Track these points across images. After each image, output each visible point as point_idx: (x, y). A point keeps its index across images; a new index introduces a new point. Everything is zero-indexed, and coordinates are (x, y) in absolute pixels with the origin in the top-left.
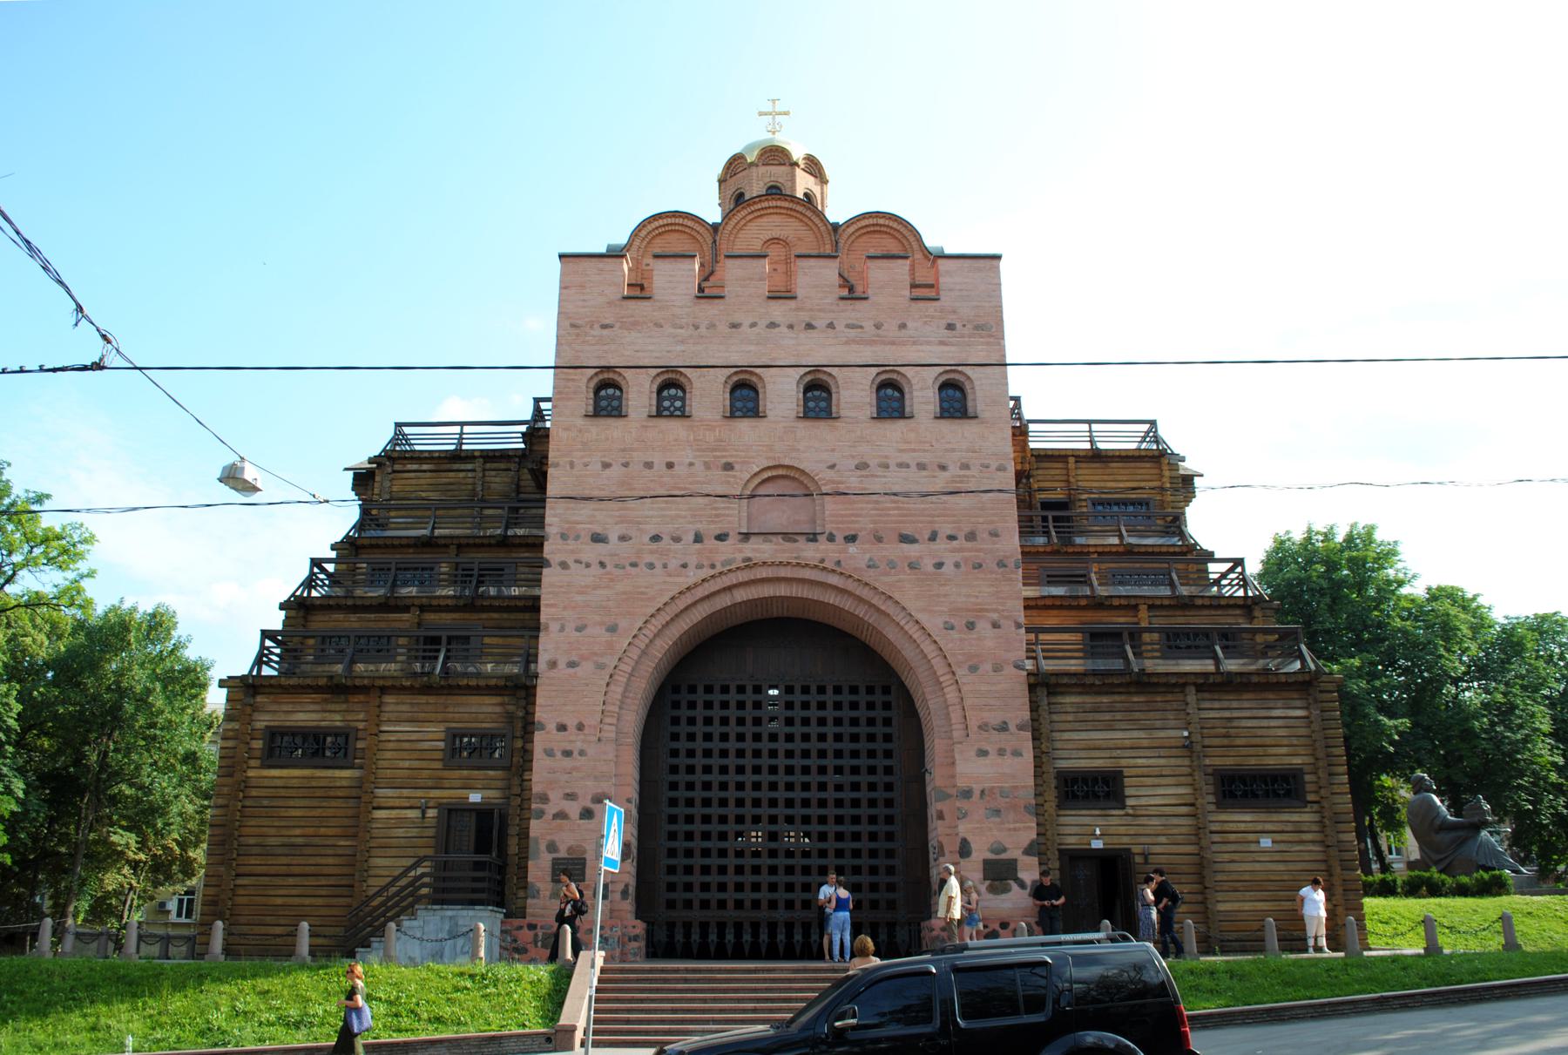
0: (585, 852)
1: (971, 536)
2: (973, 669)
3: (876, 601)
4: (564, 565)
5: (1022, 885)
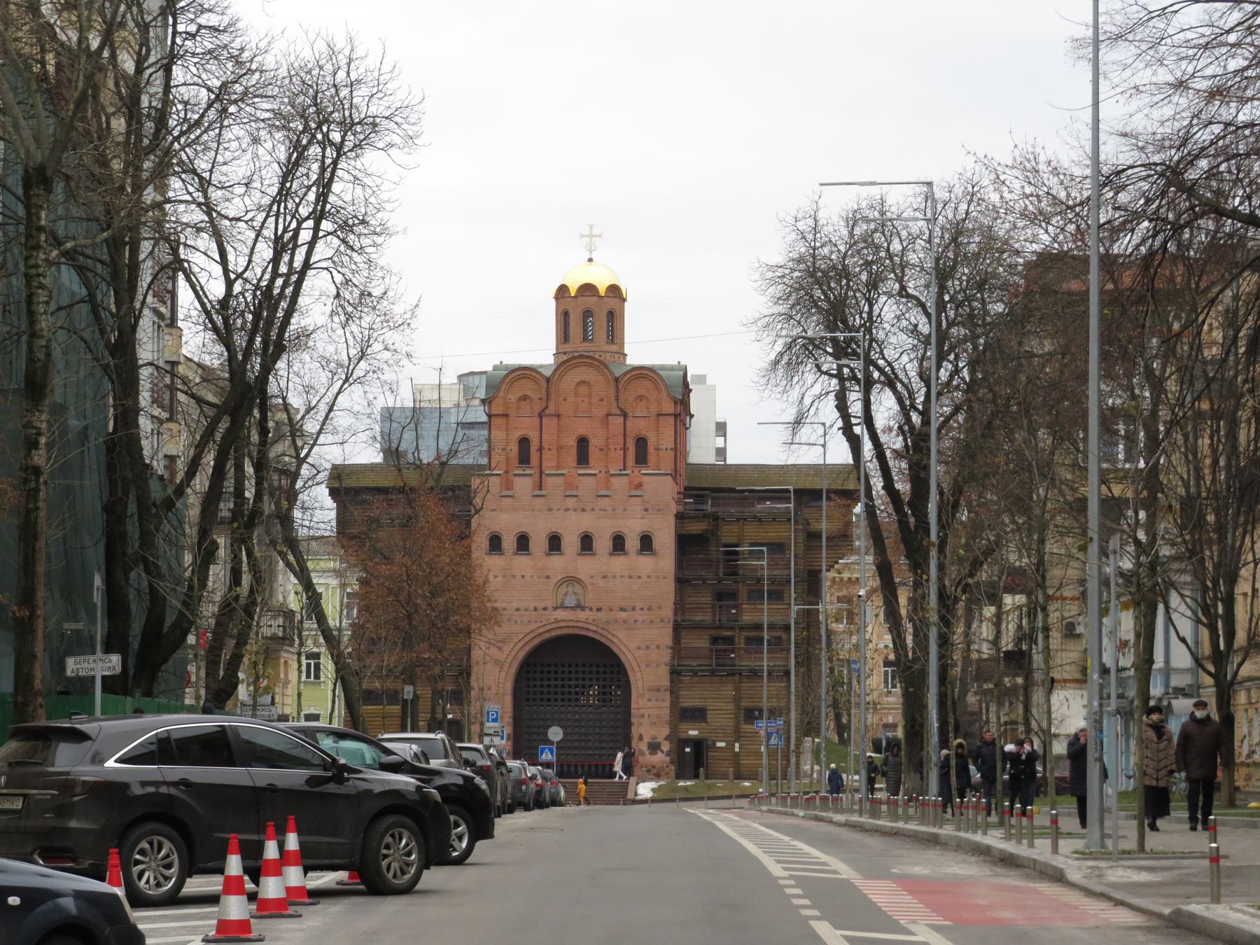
1: (650, 609)
2: (648, 666)
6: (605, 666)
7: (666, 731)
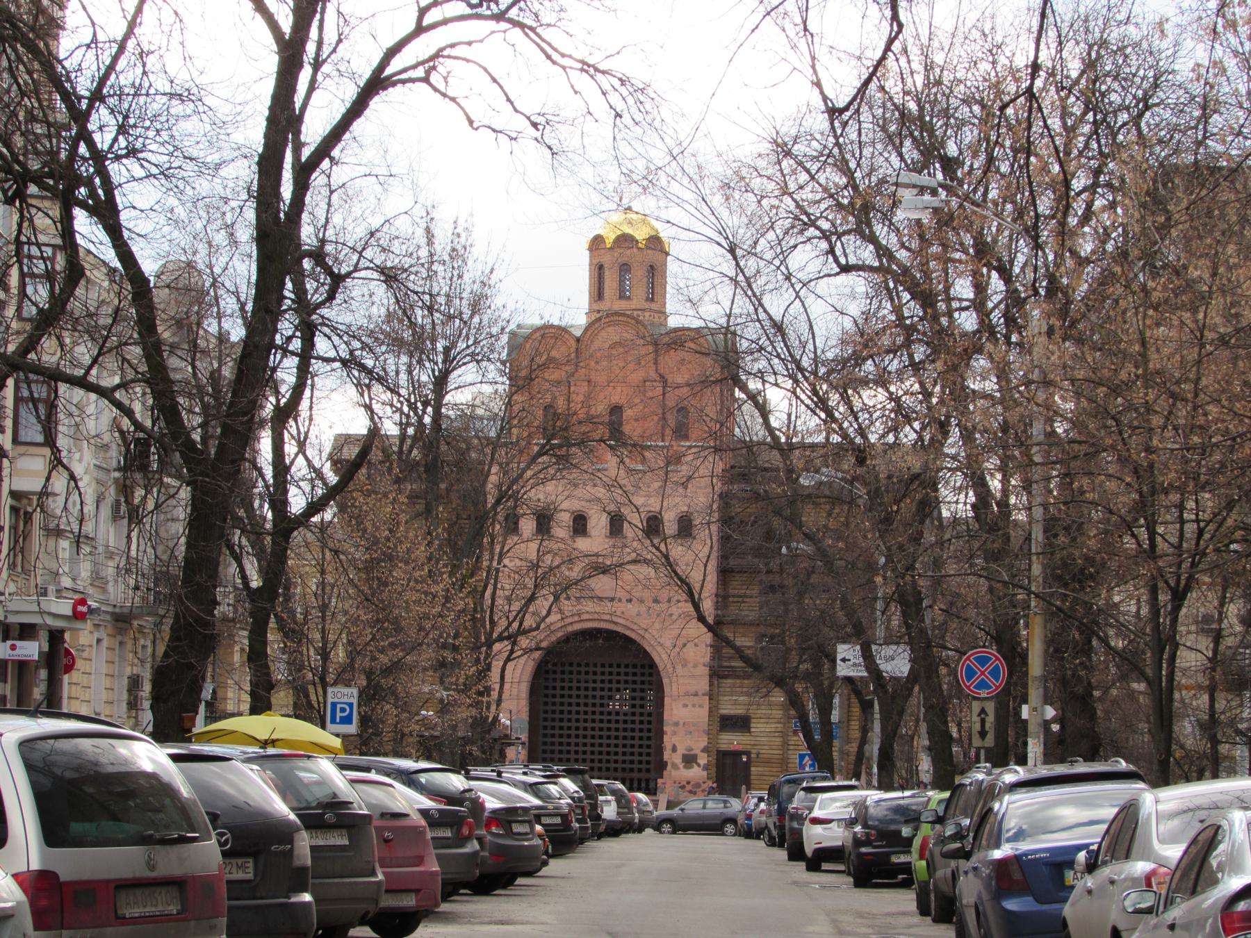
5: (699, 765)
6: (635, 666)
7: (703, 742)
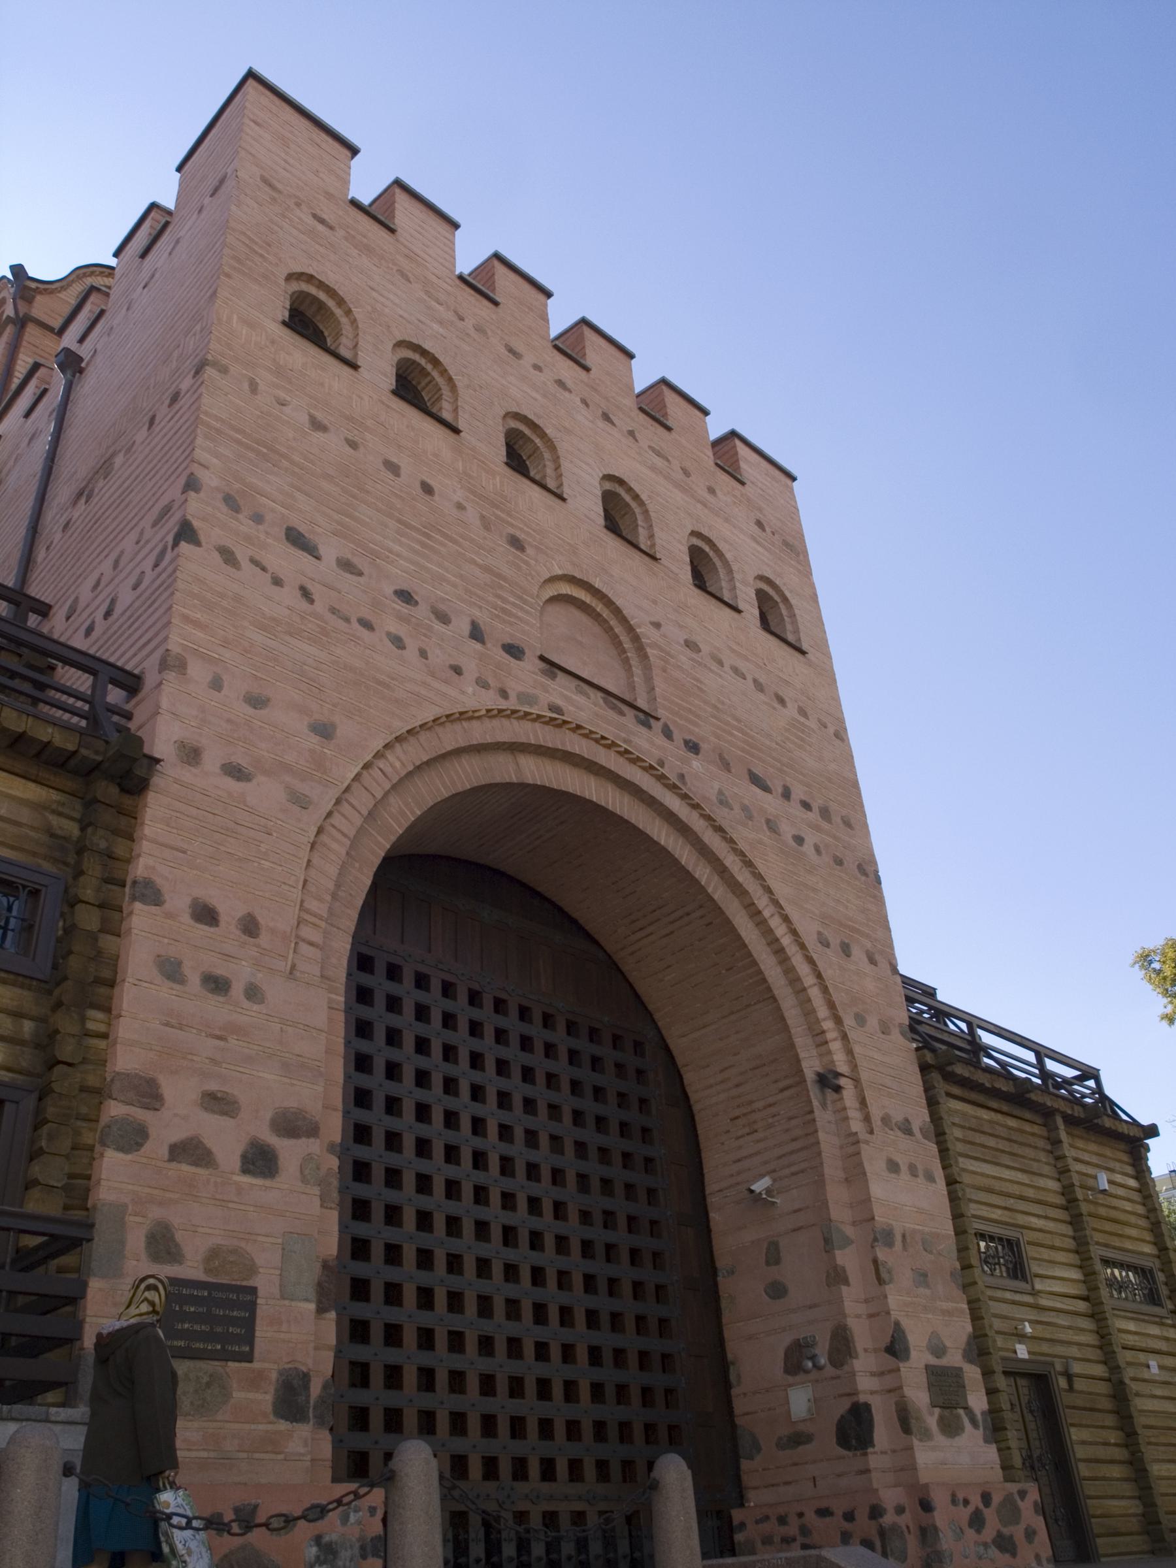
0: (252, 1270)
1: (825, 813)
3: (731, 862)
4: (228, 556)
6: (594, 1035)
